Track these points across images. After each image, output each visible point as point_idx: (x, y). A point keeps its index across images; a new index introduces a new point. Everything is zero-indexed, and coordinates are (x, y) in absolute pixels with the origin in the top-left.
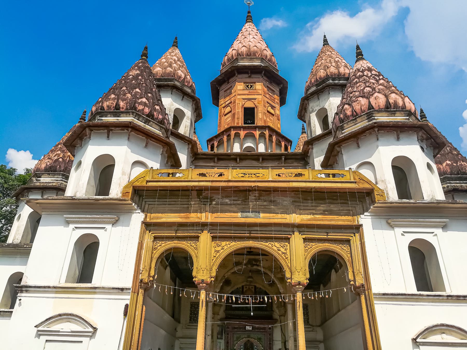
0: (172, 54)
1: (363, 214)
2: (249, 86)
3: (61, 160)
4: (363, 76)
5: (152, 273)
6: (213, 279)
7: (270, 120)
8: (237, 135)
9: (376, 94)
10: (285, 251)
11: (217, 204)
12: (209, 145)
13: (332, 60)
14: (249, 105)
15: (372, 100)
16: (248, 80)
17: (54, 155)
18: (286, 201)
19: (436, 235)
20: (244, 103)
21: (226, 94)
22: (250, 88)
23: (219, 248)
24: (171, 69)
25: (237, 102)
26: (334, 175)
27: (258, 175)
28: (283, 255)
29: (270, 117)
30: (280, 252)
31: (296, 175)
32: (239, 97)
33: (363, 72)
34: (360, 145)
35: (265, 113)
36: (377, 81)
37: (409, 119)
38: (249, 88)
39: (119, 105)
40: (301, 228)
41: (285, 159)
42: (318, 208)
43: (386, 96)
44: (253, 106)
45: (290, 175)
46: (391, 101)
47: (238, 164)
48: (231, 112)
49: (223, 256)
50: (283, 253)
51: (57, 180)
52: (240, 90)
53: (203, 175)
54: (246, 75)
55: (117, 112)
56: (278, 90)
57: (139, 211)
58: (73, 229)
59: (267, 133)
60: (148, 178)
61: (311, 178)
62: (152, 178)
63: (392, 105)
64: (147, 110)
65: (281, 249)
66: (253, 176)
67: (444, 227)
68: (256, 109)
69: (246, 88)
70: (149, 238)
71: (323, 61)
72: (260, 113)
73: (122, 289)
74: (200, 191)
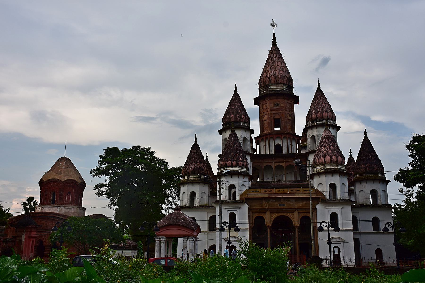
1: (317, 204)
2: (277, 105)
3: (196, 168)
4: (325, 143)
6: (271, 225)
10: (293, 216)
11: (271, 202)
12: (256, 140)
13: (320, 105)
14: (277, 117)
16: (276, 100)
17: (192, 165)
19: (339, 211)
20: (275, 116)
21: (263, 107)
22: (277, 105)
23: (273, 216)
25: (270, 115)
27: (284, 191)
28: (292, 218)
29: (289, 122)
30: (291, 217)
31: (297, 191)
33: (325, 139)
36: (330, 147)
37: (338, 167)
38: (276, 105)
39: (232, 163)
40: (298, 209)
42: (304, 202)
45: (295, 190)
47: (274, 160)
48: (267, 120)
49: (274, 218)
50: (292, 217)
51: (197, 177)
53: (265, 191)
56: (293, 101)
57: (247, 205)
58: (227, 211)
60: (247, 193)
61: (301, 192)
62: (249, 193)
63: (333, 161)
65: (292, 216)
66: (283, 191)
67: (342, 208)
68: (281, 120)
69: (275, 106)
71: (315, 105)
72: (283, 122)
73: (246, 229)
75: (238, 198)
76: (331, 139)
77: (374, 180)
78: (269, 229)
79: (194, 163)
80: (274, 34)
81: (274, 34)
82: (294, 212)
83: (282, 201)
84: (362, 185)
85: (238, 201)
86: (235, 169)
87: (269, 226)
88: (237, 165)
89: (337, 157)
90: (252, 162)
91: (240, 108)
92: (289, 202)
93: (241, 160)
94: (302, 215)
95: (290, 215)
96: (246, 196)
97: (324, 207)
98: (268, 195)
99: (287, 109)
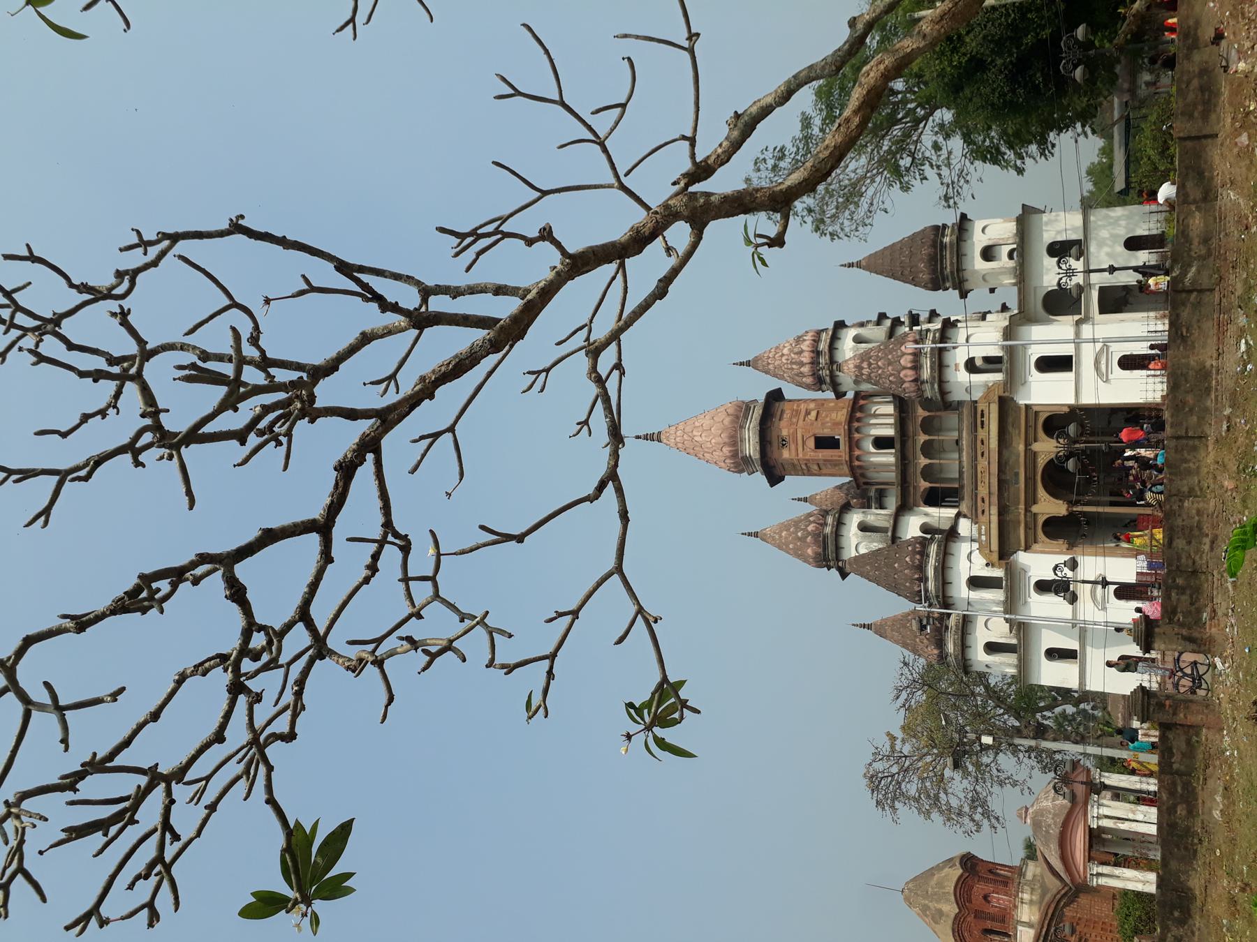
0: (777, 537)
2: (783, 443)
5: (1061, 541)
7: (827, 416)
8: (858, 459)
9: (901, 375)
15: (907, 379)
16: (775, 444)
18: (1006, 453)
23: (1043, 500)
24: (809, 538)
26: (982, 416)
31: (983, 444)
32: (801, 456)
34: (949, 390)
35: (822, 424)
37: (926, 354)
40: (1027, 444)
41: (904, 413)
43: (905, 368)
44: (812, 440)
46: (909, 365)
49: (1048, 496)
52: (790, 454)
54: (768, 449)
55: (924, 579)
59: (856, 425)
60: (988, 551)
64: (918, 557)
70: (1035, 547)
74: (1000, 514)
75: (998, 573)
76: (863, 361)
77: (959, 255)
78: (1075, 509)
79: (918, 640)
80: (638, 437)
81: (638, 437)
82: (1035, 453)
83: (1008, 478)
84: (969, 278)
85: (1006, 574)
86: (930, 572)
87: (1067, 510)
88: (921, 568)
89: (904, 354)
90: (916, 509)
91: (793, 533)
92: (1011, 463)
93: (911, 558)
94: (1041, 433)
95: (1041, 462)
96: (995, 556)
97: (1021, 387)
98: (992, 508)
99: (794, 420)
